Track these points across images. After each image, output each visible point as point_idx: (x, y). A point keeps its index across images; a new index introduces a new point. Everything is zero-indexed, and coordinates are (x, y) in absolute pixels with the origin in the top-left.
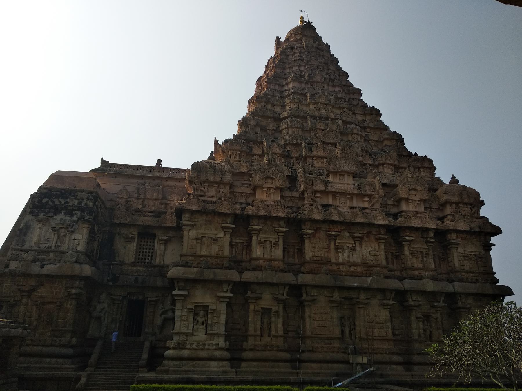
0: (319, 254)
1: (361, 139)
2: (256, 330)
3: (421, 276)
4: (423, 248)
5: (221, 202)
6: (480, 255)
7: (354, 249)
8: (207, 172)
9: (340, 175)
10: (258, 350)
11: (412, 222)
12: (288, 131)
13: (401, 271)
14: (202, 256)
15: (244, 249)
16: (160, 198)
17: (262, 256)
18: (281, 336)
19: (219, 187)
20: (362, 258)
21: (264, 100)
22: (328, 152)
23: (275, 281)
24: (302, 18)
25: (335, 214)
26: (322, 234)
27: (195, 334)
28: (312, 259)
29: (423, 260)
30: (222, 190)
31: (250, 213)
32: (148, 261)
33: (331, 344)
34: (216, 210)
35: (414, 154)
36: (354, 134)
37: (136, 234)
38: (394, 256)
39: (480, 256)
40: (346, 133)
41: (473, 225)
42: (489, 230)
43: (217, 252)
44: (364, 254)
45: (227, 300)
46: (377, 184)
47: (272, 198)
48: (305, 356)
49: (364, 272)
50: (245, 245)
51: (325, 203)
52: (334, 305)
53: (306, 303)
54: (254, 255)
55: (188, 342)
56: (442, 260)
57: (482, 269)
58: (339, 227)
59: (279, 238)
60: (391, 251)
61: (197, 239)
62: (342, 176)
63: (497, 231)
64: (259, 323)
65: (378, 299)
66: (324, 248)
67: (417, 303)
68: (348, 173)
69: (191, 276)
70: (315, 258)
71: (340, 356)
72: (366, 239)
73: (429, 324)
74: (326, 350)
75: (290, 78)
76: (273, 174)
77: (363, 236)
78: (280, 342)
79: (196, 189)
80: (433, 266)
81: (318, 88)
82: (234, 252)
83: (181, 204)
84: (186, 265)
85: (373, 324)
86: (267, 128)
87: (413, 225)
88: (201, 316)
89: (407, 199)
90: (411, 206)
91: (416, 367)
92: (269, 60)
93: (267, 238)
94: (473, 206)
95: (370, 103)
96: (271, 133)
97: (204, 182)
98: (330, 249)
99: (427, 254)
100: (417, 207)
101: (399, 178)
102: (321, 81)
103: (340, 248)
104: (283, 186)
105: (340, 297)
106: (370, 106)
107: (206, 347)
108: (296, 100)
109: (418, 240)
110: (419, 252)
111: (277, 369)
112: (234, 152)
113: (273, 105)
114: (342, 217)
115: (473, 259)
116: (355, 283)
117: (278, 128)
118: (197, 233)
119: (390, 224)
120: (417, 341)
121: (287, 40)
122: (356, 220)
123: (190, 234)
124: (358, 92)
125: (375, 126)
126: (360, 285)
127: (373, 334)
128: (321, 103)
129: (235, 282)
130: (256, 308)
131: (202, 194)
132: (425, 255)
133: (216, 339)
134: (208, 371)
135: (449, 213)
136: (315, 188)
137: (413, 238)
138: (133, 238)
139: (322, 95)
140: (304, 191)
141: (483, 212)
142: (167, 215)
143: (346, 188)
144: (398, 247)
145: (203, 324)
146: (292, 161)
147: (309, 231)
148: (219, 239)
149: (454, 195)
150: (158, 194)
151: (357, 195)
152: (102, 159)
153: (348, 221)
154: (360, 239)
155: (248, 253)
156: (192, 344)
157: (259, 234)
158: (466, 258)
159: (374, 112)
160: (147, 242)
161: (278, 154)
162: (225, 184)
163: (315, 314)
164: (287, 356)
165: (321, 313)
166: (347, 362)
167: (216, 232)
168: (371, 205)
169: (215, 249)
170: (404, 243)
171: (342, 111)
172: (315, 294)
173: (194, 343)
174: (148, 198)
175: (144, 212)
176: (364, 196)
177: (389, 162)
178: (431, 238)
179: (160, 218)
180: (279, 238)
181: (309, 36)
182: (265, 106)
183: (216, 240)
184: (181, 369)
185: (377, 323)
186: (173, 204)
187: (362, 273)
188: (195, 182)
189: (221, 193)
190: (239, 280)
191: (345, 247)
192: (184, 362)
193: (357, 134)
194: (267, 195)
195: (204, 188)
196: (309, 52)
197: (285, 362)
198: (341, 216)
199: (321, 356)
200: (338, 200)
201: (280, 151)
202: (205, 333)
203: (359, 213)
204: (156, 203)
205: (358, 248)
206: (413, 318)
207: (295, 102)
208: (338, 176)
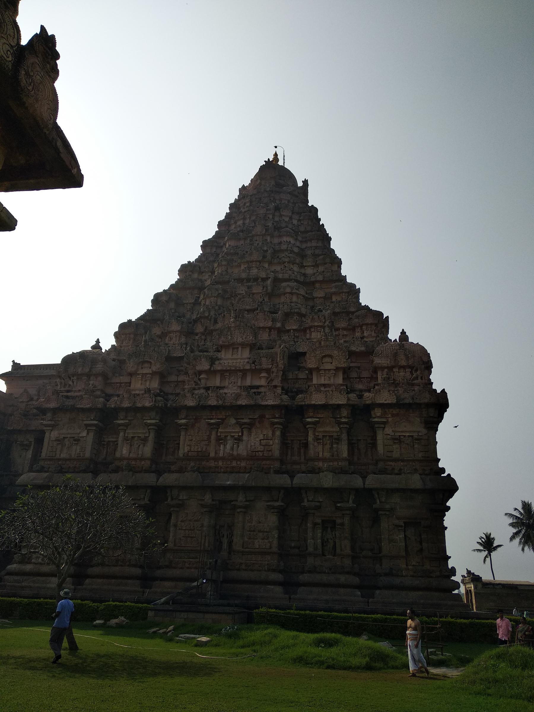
7: (239, 439)
9: (233, 349)
14: (59, 460)
25: (212, 398)
29: (332, 448)
33: (196, 558)
36: (287, 293)
37: (32, 440)
38: (301, 445)
44: (252, 444)
48: (159, 573)
54: (118, 455)
56: (370, 445)
57: (420, 455)
59: (149, 432)
60: (299, 439)
61: (59, 440)
62: (235, 350)
70: (190, 454)
74: (188, 565)
80: (345, 454)
85: (255, 533)
87: (313, 402)
89: (318, 369)
90: (323, 378)
96: (188, 307)
99: (338, 440)
104: (160, 370)
105: (213, 500)
109: (328, 421)
114: (221, 400)
116: (228, 481)
123: (52, 435)
136: (198, 368)
137: (318, 419)
139: (254, 251)
146: (197, 338)
147: (183, 421)
152: (13, 361)
154: (249, 427)
158: (395, 441)
161: (177, 331)
162: (97, 375)
163: (182, 521)
169: (75, 451)
172: (185, 498)
176: (261, 371)
177: (316, 324)
180: (149, 432)
183: (78, 440)
185: (260, 531)
187: (245, 468)
189: (90, 385)
191: (229, 437)
193: (291, 293)
194: (141, 384)
198: (219, 399)
200: (227, 380)
201: (179, 328)
203: (243, 393)
205: (245, 438)
206: (309, 525)
208: (231, 350)
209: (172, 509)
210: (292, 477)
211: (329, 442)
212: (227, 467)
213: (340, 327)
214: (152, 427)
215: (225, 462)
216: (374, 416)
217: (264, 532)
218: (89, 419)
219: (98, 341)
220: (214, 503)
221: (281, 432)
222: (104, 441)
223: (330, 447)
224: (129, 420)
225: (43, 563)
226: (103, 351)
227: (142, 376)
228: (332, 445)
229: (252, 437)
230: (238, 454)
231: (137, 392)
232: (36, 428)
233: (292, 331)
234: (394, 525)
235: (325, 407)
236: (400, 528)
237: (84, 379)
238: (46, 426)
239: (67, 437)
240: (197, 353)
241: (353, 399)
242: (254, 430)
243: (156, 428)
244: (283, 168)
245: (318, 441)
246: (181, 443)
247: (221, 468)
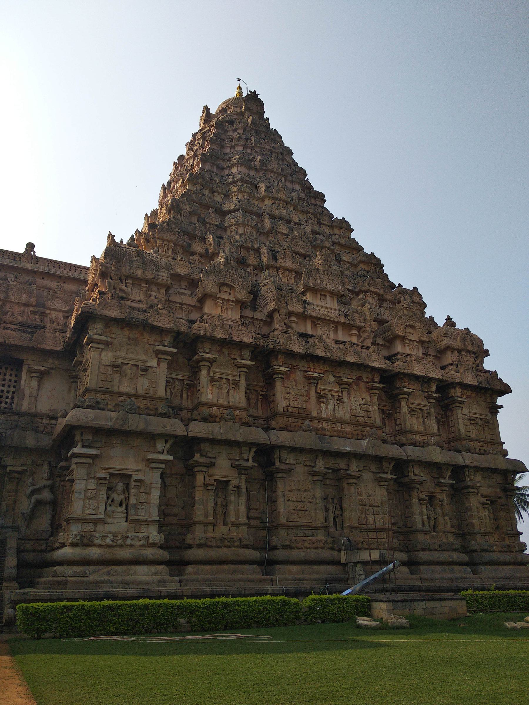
0: (296, 404)
2: (206, 515)
3: (424, 442)
4: (425, 406)
5: (156, 310)
6: (486, 419)
7: (340, 400)
8: (132, 261)
10: (211, 547)
11: (414, 367)
12: (238, 229)
13: (395, 436)
14: (122, 394)
15: (185, 389)
16: (34, 303)
17: (215, 401)
18: (244, 525)
20: (351, 413)
21: (200, 181)
22: (298, 264)
23: (239, 438)
24: (240, 88)
25: (319, 347)
26: (298, 375)
27: (109, 520)
28: (286, 410)
29: (424, 422)
30: (154, 294)
31: (202, 333)
32: (6, 406)
33: (313, 536)
34: (150, 320)
35: (397, 285)
36: (325, 247)
39: (487, 421)
40: (315, 245)
41: (481, 379)
42: (498, 387)
43: (146, 390)
44: (354, 408)
45: (163, 466)
46: (367, 313)
47: (230, 316)
48: (280, 554)
49: (355, 433)
50: (187, 384)
51: (302, 331)
52: (317, 478)
53: (280, 475)
54: (204, 399)
55: (97, 535)
56: (442, 423)
62: (323, 297)
63: (506, 390)
64: (211, 504)
65: (372, 472)
66: (301, 395)
67: (421, 479)
68: (332, 294)
69: (108, 424)
70: (290, 409)
71: (327, 554)
72: (354, 385)
73: (432, 509)
75: (235, 159)
76: (233, 281)
77: (353, 382)
78: (242, 533)
79: (112, 287)
80: (436, 430)
81: (273, 179)
82: (168, 394)
83: (91, 305)
84: (95, 406)
85: (367, 507)
86: (207, 220)
87: (415, 372)
88: (119, 492)
89: (403, 338)
91: (423, 568)
92: (194, 135)
93: (222, 373)
94: (476, 355)
95: (338, 215)
98: (309, 398)
100: (415, 350)
101: (387, 311)
102: (278, 171)
103: (324, 397)
104: (246, 300)
106: (337, 218)
107: (129, 542)
108: (246, 190)
111: (249, 576)
112: (166, 242)
113: (212, 191)
114: (329, 352)
115: (479, 423)
117: (222, 223)
119: (388, 368)
120: (421, 531)
121: (223, 110)
122: (346, 358)
124: (321, 197)
125: (347, 244)
126: (354, 450)
127: (366, 522)
128: (280, 200)
129: (176, 437)
130: (207, 480)
131: (124, 295)
132: (427, 415)
133: (143, 529)
134: (134, 582)
135: (451, 362)
137: (413, 390)
140: (275, 310)
141: (488, 364)
142: (47, 330)
143: (329, 314)
144: (390, 403)
145: (121, 505)
147: (284, 369)
148: (150, 369)
149: (456, 339)
150: (30, 296)
151: (344, 324)
153: (336, 358)
154: (347, 386)
155: (190, 397)
156: (103, 537)
157: (212, 366)
159: (344, 225)
160: (5, 375)
162: (159, 286)
164: (255, 554)
165: (299, 490)
166: (337, 563)
167: (145, 358)
168: (360, 341)
170: (401, 396)
171: (305, 216)
172: (292, 462)
173: (107, 536)
174: (13, 300)
175: (5, 322)
177: (373, 289)
178: (432, 392)
179: (35, 335)
181: (254, 111)
182: (201, 189)
183: (145, 370)
184: (88, 579)
186: (55, 315)
188: (112, 275)
189: (153, 298)
190: (186, 434)
192: (92, 568)
193: (329, 249)
194: (222, 311)
195: (126, 286)
196: (257, 131)
197: (250, 565)
199: (301, 554)
202: (125, 521)
204: (26, 310)
205: (345, 399)
206: (415, 500)
207: (245, 192)
213: (388, 299)
214: (243, 369)
215: (329, 425)
232: (5, 341)
237: (143, 287)
239: (128, 364)
242: (353, 392)
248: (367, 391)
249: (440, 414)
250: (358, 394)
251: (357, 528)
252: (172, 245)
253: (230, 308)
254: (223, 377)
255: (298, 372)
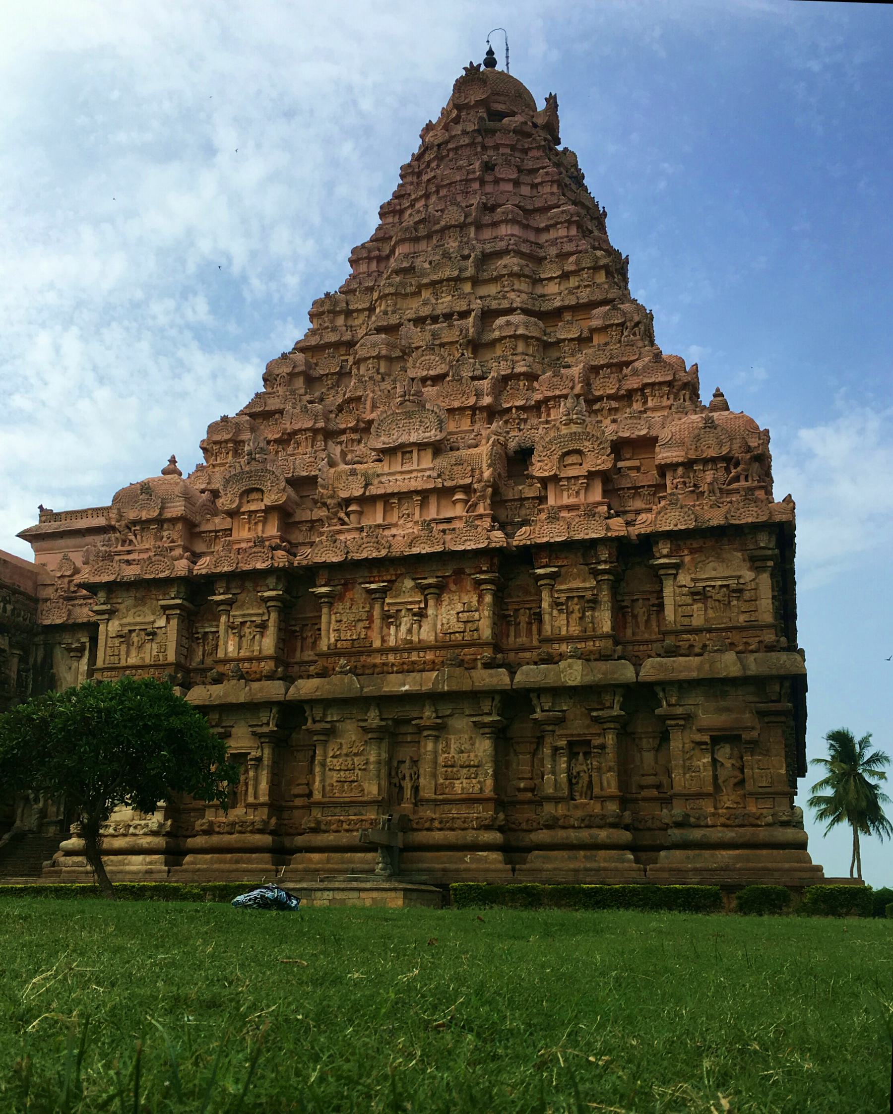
1: (528, 345)
4: (586, 589)
7: (421, 615)
9: (404, 453)
19: (161, 528)
28: (332, 647)
54: (221, 654)
56: (655, 608)
58: (392, 571)
60: (528, 606)
61: (121, 636)
62: (408, 455)
66: (359, 620)
72: (453, 587)
80: (606, 627)
85: (455, 769)
87: (545, 540)
89: (555, 479)
90: (565, 494)
93: (244, 616)
97: (135, 523)
99: (594, 603)
105: (382, 720)
110: (576, 599)
116: (404, 685)
118: (121, 625)
131: (130, 548)
136: (344, 494)
137: (556, 569)
138: (81, 650)
147: (323, 590)
148: (158, 631)
151: (434, 490)
154: (437, 591)
163: (333, 757)
167: (151, 618)
169: (150, 653)
172: (335, 719)
177: (557, 393)
183: (154, 634)
185: (462, 767)
187: (434, 662)
194: (249, 528)
195: (135, 535)
200: (396, 511)
205: (430, 611)
206: (547, 751)
208: (399, 455)
209: (315, 738)
210: (512, 673)
211: (578, 607)
212: (404, 663)
216: (658, 555)
217: (469, 766)
218: (167, 597)
219: (173, 461)
220: (383, 723)
221: (495, 596)
222: (198, 633)
223: (580, 615)
224: (234, 594)
225: (116, 834)
226: (184, 476)
227: (250, 516)
228: (584, 614)
229: (443, 609)
230: (420, 641)
231: (244, 545)
233: (514, 410)
234: (693, 742)
235: (569, 546)
236: (704, 747)
238: (98, 613)
239: (135, 630)
240: (343, 467)
241: (617, 528)
242: (445, 597)
243: (279, 604)
244: (505, 77)
245: (559, 608)
246: (323, 626)
247: (393, 665)
248: (475, 589)
249: (653, 592)
250: (456, 598)
251: (428, 801)
252: (230, 445)
253: (259, 521)
254: (245, 619)
255: (358, 586)
